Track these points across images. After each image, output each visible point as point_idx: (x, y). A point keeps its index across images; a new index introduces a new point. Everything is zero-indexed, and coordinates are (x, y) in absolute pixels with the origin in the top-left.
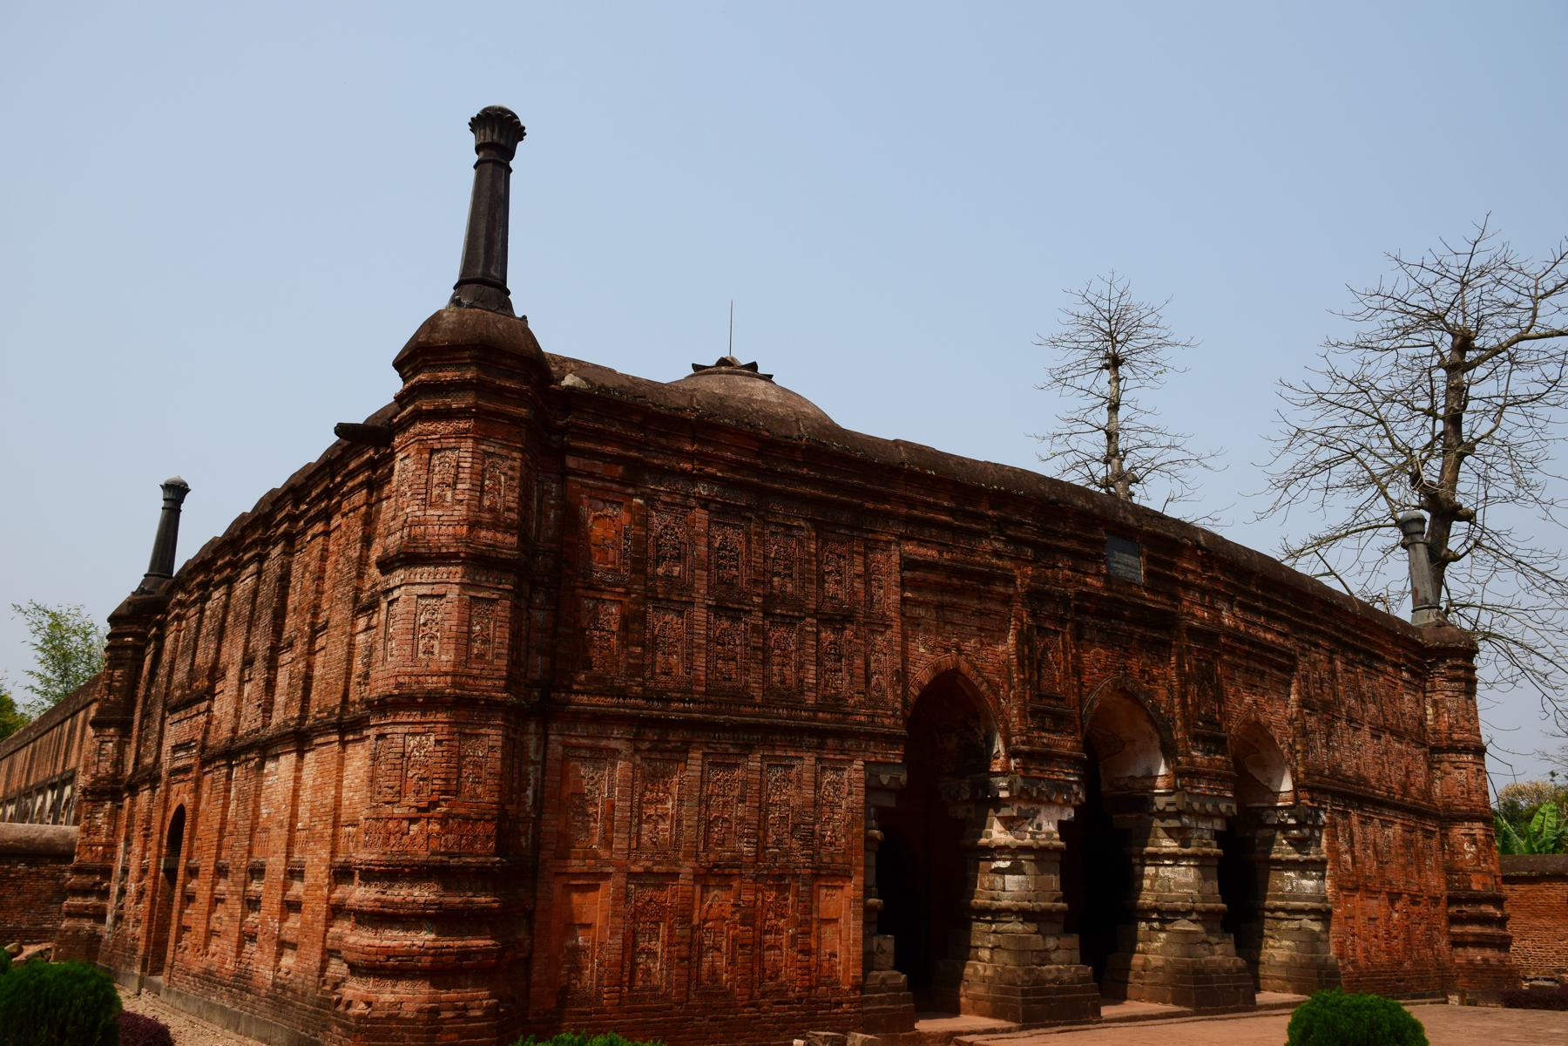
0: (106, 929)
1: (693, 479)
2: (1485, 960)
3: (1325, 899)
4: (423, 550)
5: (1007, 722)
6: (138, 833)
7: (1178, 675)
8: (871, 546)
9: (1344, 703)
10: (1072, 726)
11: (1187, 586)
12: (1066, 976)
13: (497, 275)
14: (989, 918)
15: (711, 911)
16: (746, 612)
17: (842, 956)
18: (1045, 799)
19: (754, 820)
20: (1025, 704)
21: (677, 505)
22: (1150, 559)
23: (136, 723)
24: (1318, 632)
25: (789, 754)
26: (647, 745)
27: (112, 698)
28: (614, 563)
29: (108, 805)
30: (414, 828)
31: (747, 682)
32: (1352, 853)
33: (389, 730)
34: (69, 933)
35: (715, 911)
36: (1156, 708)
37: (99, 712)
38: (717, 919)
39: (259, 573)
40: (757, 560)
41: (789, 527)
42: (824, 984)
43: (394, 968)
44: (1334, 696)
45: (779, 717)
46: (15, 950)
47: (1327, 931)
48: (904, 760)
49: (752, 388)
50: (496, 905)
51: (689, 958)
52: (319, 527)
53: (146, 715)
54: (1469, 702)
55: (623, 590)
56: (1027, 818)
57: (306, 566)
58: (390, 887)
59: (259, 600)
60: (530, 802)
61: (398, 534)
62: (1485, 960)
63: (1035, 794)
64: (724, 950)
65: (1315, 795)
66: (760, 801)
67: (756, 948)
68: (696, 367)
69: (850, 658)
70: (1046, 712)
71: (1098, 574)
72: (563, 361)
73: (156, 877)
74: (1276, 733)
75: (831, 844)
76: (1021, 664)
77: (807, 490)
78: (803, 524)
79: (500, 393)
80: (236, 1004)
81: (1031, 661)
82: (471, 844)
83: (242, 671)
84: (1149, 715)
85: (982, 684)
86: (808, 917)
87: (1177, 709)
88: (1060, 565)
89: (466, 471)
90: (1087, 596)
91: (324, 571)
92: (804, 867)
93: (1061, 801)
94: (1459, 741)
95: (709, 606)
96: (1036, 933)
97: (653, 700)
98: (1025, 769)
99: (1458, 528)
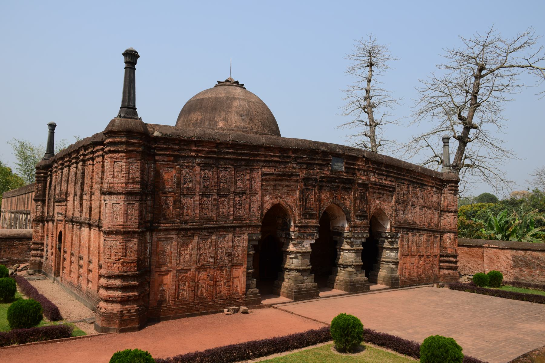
0: (44, 260)
1: (195, 158)
2: (449, 273)
3: (397, 259)
4: (113, 191)
5: (295, 217)
6: (50, 235)
7: (353, 198)
8: (252, 171)
9: (411, 200)
10: (316, 216)
11: (359, 170)
12: (309, 287)
13: (132, 105)
14: (288, 271)
15: (201, 278)
16: (211, 195)
17: (240, 286)
18: (306, 238)
19: (213, 253)
20: (300, 212)
21: (190, 166)
22: (346, 163)
23: (47, 201)
24: (405, 179)
25: (224, 233)
26: (181, 235)
27: (39, 192)
28: (171, 185)
29: (41, 224)
30: (115, 265)
31: (212, 215)
32: (408, 245)
33: (107, 239)
34: (33, 261)
35: (202, 278)
36: (345, 208)
37: (36, 197)
38: (203, 280)
39: (77, 167)
40: (215, 179)
41: (226, 168)
42: (234, 294)
43: (111, 301)
44: (408, 198)
45: (222, 224)
46: (18, 266)
47: (397, 268)
48: (260, 232)
49: (235, 93)
50: (137, 284)
51: (194, 290)
52: (91, 162)
53: (49, 199)
54: (455, 197)
55: (173, 193)
56: (300, 244)
57: (88, 172)
58: (109, 280)
59: (77, 176)
60: (148, 253)
61: (107, 185)
62: (449, 273)
63: (302, 237)
64: (205, 287)
65: (397, 229)
66: (215, 248)
67: (214, 286)
68: (219, 82)
69: (244, 205)
70: (307, 214)
71: (328, 170)
72: (153, 126)
73: (56, 250)
74: (386, 211)
75: (237, 257)
76: (300, 200)
77: (232, 156)
78: (230, 166)
79: (133, 144)
80: (78, 293)
81: (304, 199)
82: (130, 269)
83: (74, 197)
84: (343, 210)
85: (287, 207)
86: (230, 277)
87: (352, 208)
89: (124, 168)
90: (324, 177)
91: (93, 176)
92: (229, 264)
93: (311, 238)
94: (450, 209)
95: (200, 195)
96: (301, 275)
97: (183, 223)
98: (299, 230)
99: (472, 131)
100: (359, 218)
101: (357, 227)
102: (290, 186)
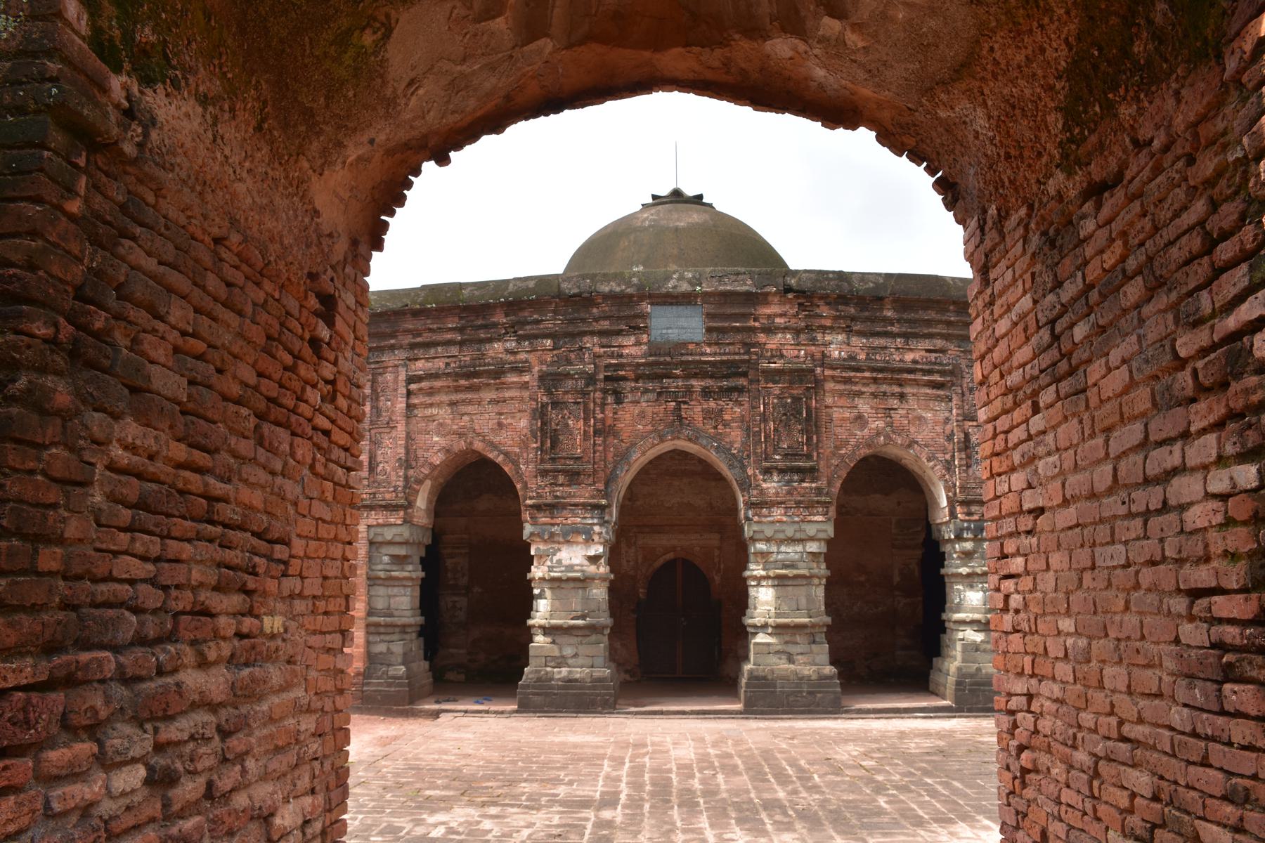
18: (561, 540)
22: (710, 316)
63: (546, 537)
65: (974, 508)
71: (638, 343)
88: (588, 345)
90: (620, 366)
100: (776, 479)
101: (771, 505)
102: (504, 401)
